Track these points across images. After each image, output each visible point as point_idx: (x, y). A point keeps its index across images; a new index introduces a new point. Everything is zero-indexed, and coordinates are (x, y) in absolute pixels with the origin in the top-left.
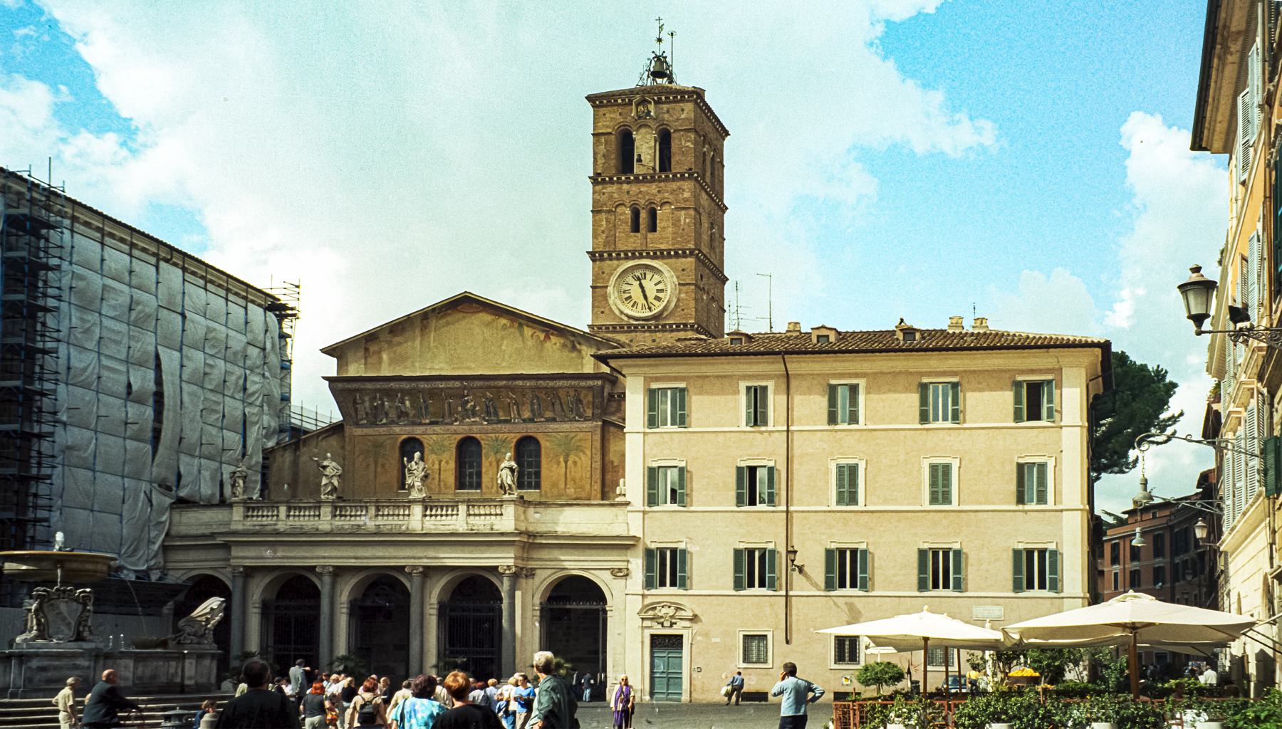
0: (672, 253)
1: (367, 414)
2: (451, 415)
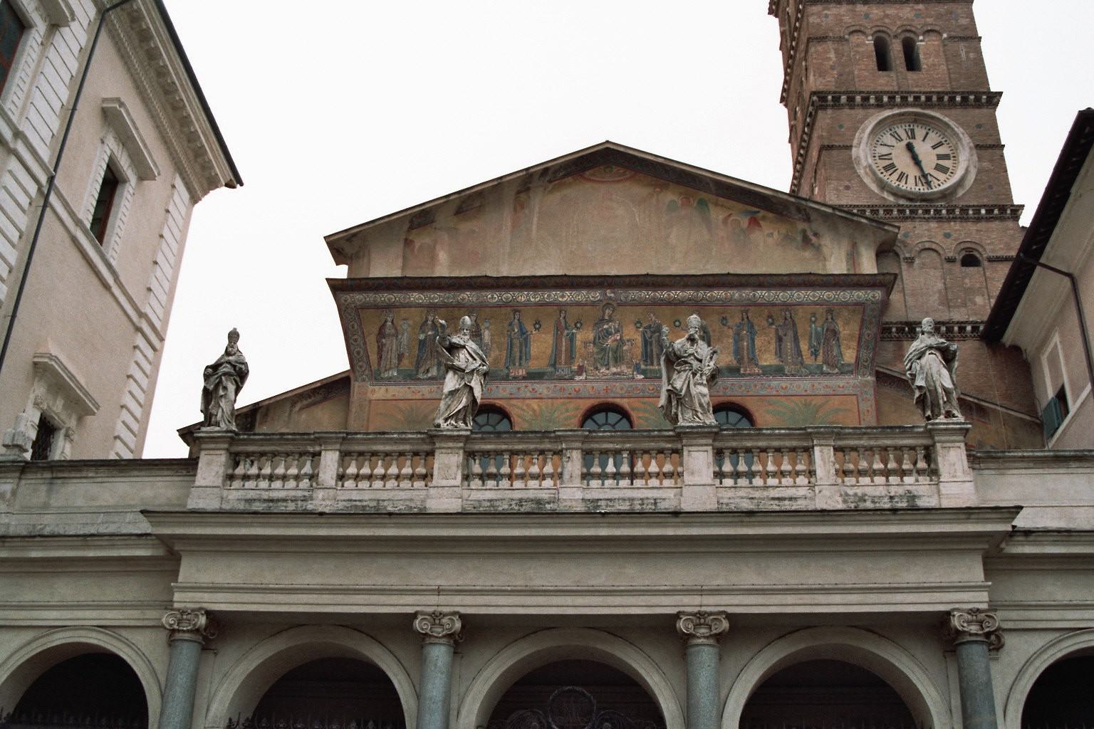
0: (958, 99)
1: (400, 357)
2: (571, 357)
